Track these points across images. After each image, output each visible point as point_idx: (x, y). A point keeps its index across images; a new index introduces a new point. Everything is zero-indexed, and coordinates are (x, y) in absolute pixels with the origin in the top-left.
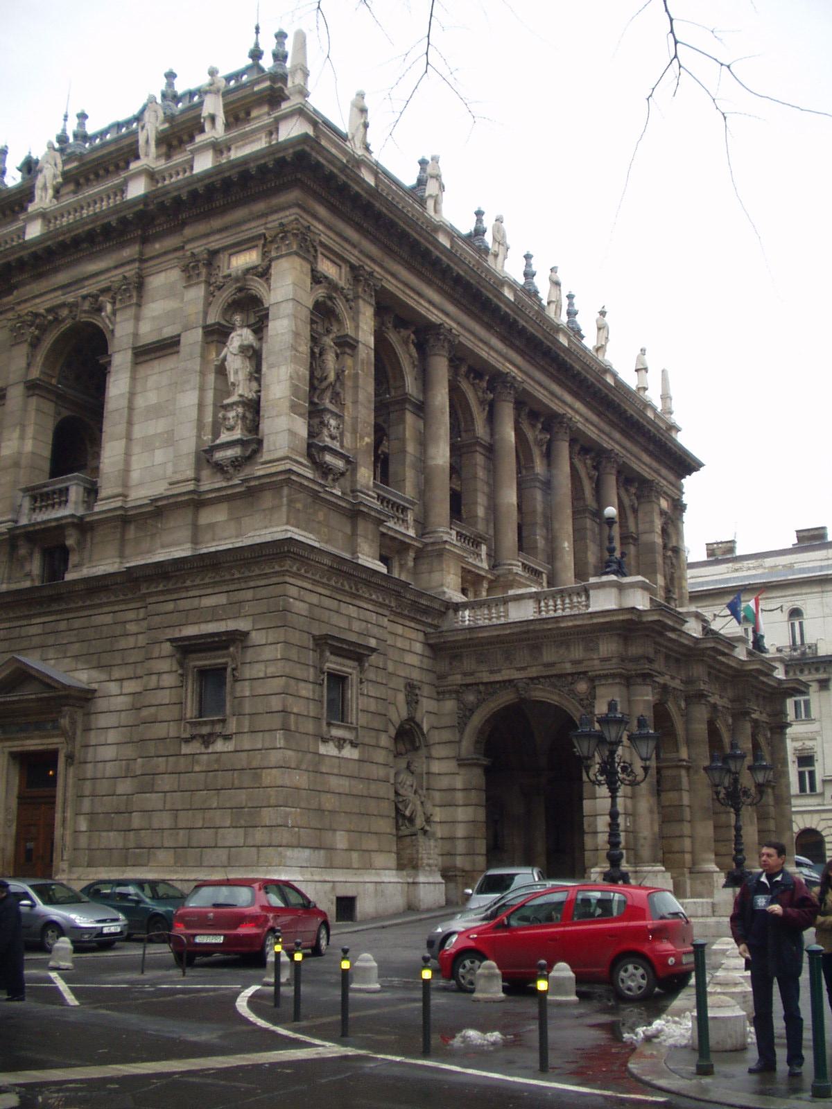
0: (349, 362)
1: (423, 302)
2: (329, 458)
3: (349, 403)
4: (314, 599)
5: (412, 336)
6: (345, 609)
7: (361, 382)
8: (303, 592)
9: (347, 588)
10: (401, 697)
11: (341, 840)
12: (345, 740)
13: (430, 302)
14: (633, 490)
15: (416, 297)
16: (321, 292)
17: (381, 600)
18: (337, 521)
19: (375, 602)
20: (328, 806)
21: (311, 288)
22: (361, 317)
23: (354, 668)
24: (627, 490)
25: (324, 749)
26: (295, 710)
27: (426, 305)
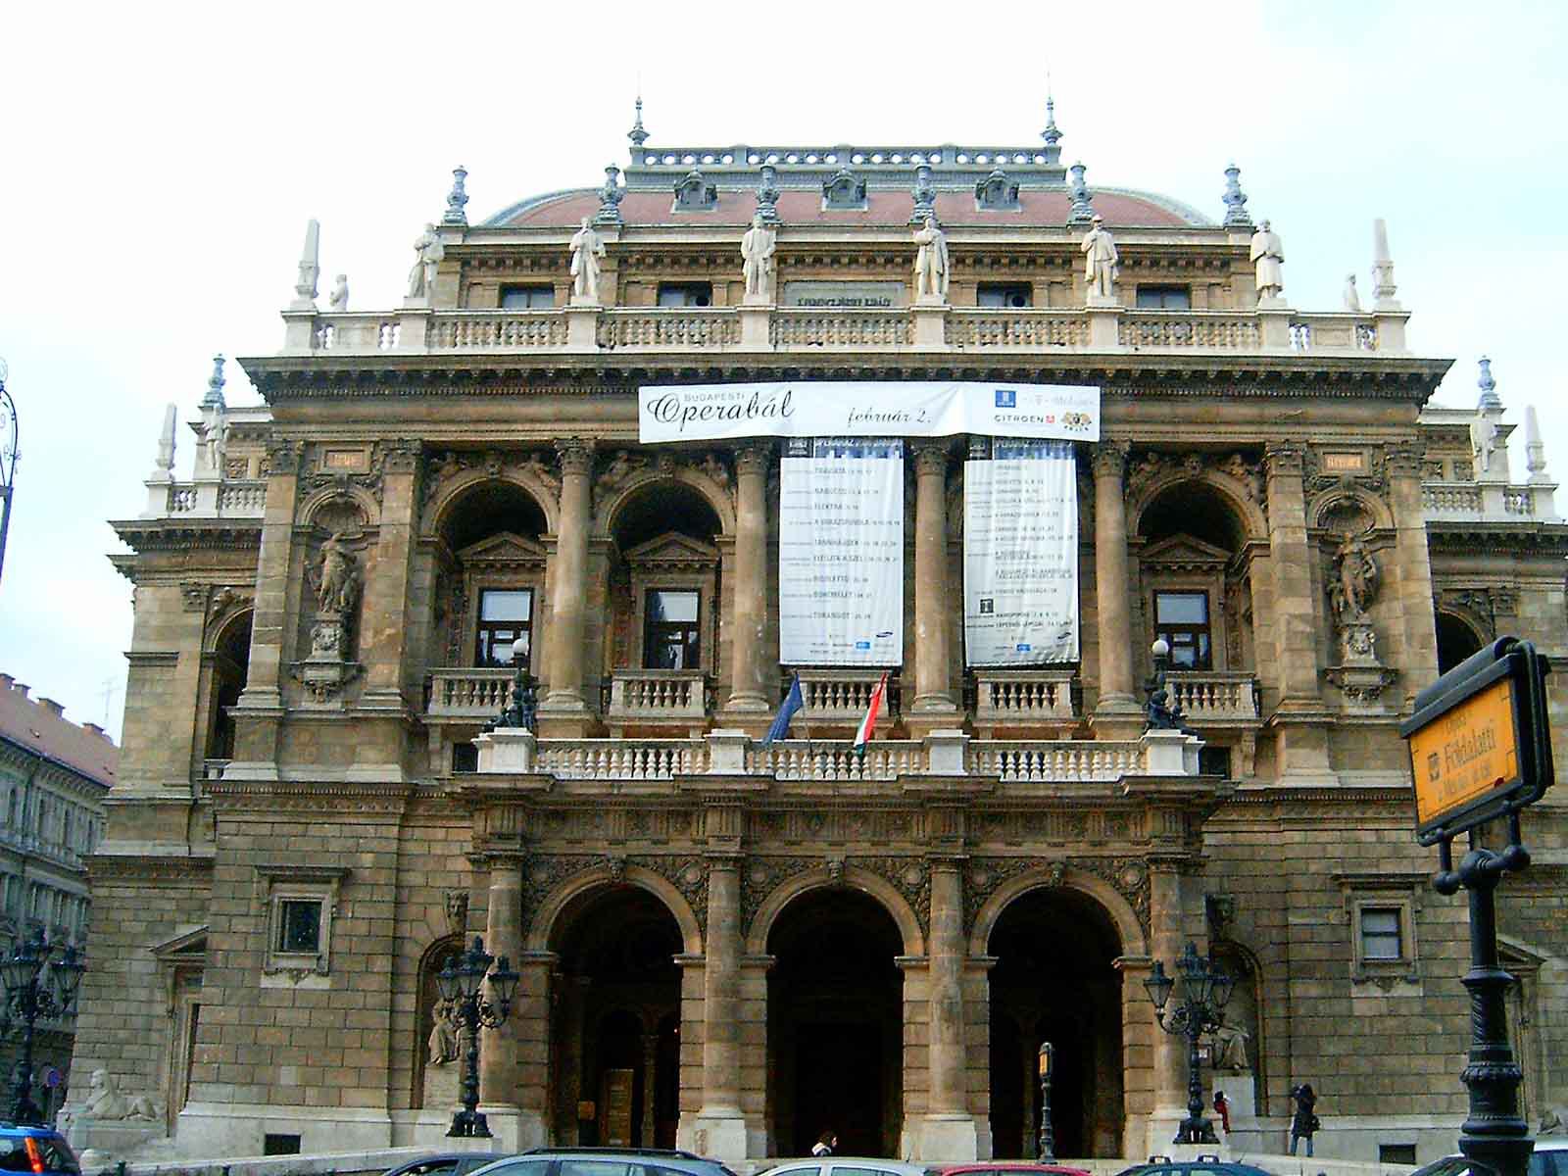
0: (376, 551)
1: (514, 427)
2: (310, 674)
3: (369, 596)
4: (265, 829)
5: (537, 466)
6: (313, 830)
7: (380, 568)
8: (244, 826)
9: (315, 808)
10: (436, 913)
11: (288, 1076)
12: (300, 971)
13: (533, 421)
14: (1238, 470)
15: (505, 427)
16: (325, 495)
17: (378, 809)
18: (328, 736)
19: (368, 815)
20: (269, 1041)
21: (299, 500)
22: (386, 497)
23: (325, 892)
24: (1230, 474)
25: (266, 982)
26: (225, 947)
27: (527, 427)
